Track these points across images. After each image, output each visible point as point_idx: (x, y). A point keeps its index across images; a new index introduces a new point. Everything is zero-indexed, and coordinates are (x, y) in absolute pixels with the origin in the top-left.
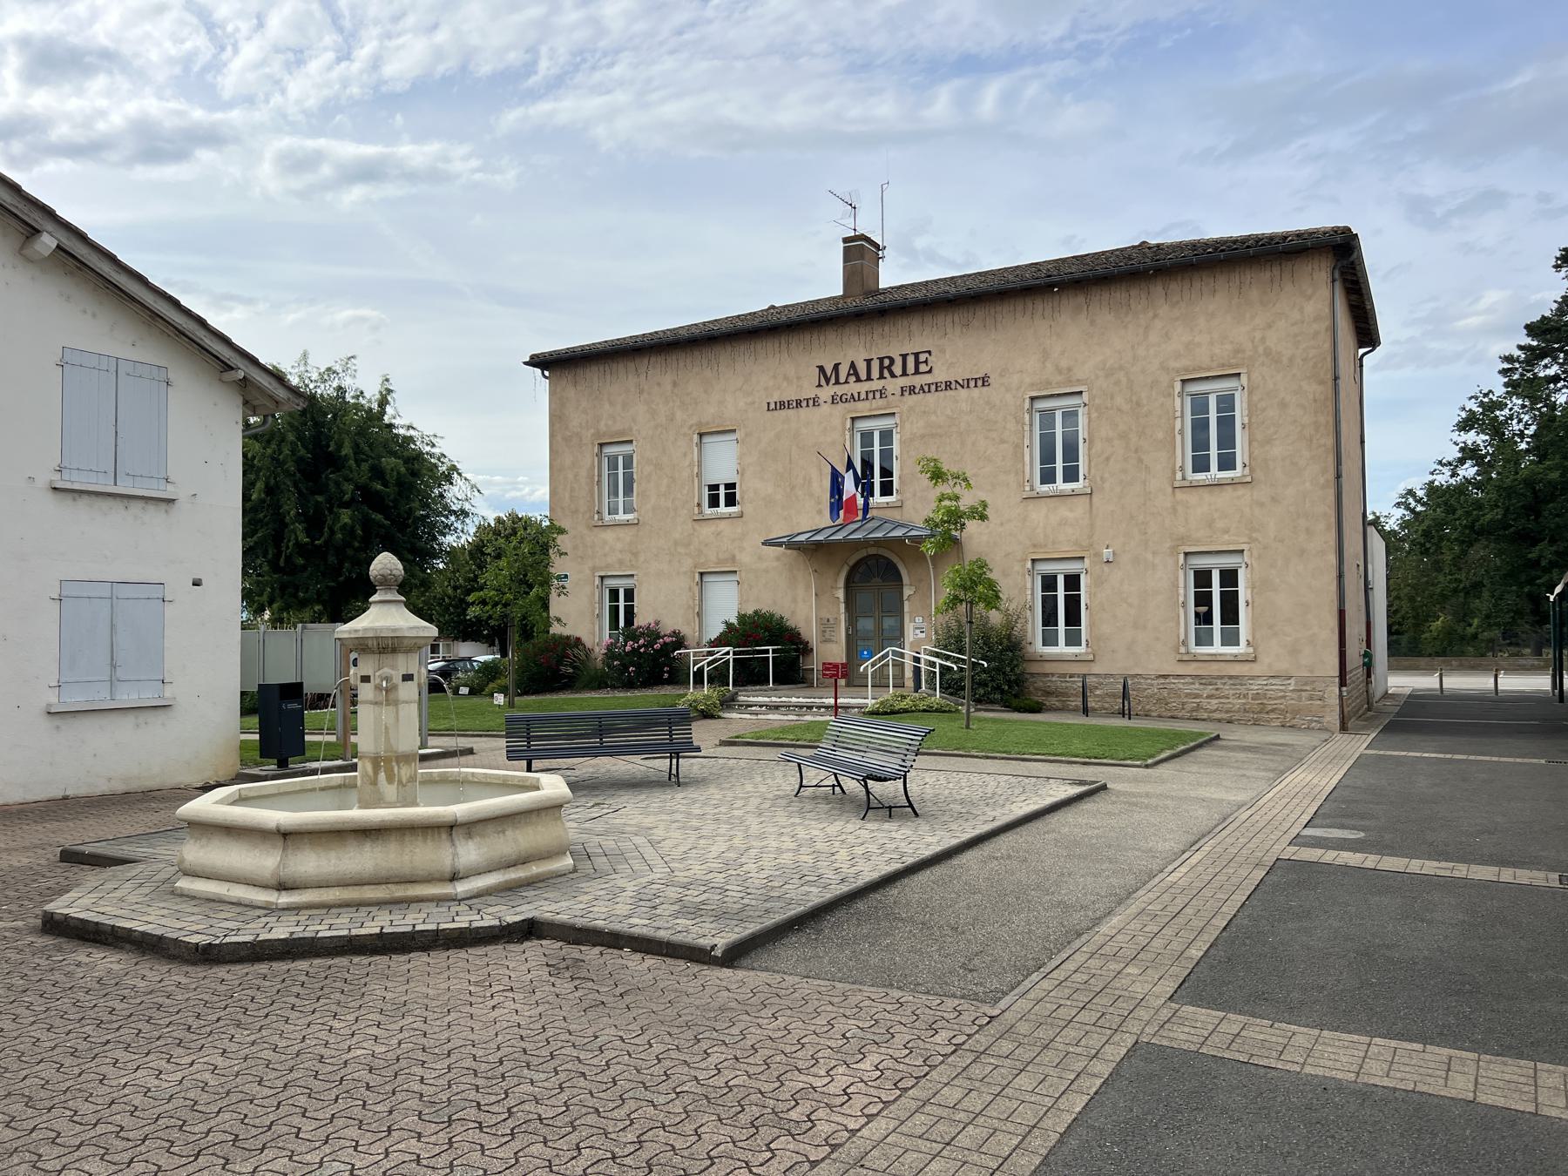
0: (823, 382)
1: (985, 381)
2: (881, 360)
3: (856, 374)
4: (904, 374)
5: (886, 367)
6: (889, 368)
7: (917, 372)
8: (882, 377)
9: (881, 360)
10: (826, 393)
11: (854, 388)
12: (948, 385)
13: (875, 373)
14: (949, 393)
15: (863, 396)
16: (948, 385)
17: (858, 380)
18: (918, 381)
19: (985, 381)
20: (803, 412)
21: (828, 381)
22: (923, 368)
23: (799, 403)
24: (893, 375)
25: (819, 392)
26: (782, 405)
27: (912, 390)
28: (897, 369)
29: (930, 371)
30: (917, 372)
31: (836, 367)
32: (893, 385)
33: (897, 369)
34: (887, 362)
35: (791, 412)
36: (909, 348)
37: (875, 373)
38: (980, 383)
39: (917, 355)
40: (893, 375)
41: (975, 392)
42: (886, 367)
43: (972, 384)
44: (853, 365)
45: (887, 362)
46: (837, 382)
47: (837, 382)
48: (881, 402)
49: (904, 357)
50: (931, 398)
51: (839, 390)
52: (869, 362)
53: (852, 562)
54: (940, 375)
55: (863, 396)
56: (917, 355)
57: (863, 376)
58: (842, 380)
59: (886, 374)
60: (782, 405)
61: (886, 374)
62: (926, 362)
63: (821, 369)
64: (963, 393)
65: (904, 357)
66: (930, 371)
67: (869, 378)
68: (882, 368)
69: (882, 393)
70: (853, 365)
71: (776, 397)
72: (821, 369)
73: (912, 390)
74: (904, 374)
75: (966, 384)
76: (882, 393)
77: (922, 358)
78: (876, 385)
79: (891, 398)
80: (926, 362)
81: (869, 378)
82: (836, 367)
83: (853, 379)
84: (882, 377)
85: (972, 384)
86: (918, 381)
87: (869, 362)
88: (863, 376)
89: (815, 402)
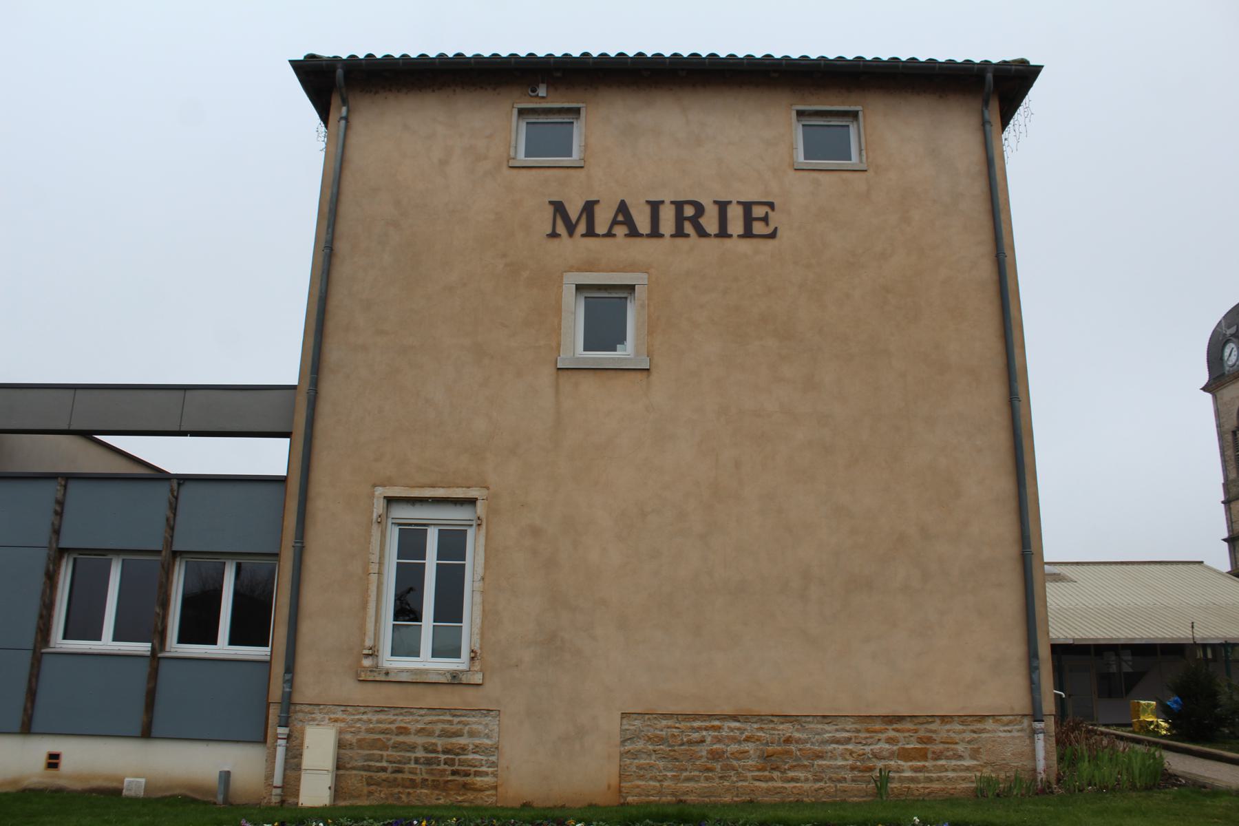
0: (561, 229)
2: (679, 206)
3: (629, 222)
6: (695, 221)
7: (748, 234)
8: (679, 233)
9: (679, 206)
17: (634, 233)
21: (571, 228)
22: (758, 228)
24: (702, 233)
28: (710, 222)
30: (748, 234)
33: (710, 222)
34: (689, 211)
39: (747, 207)
40: (702, 233)
44: (623, 208)
45: (689, 211)
47: (590, 233)
49: (723, 206)
52: (655, 206)
56: (747, 207)
57: (643, 225)
58: (601, 228)
59: (688, 228)
61: (688, 228)
62: (765, 219)
65: (723, 206)
66: (773, 235)
68: (680, 219)
70: (623, 208)
72: (559, 208)
77: (758, 212)
83: (620, 231)
84: (679, 233)
87: (655, 206)
88: (643, 225)
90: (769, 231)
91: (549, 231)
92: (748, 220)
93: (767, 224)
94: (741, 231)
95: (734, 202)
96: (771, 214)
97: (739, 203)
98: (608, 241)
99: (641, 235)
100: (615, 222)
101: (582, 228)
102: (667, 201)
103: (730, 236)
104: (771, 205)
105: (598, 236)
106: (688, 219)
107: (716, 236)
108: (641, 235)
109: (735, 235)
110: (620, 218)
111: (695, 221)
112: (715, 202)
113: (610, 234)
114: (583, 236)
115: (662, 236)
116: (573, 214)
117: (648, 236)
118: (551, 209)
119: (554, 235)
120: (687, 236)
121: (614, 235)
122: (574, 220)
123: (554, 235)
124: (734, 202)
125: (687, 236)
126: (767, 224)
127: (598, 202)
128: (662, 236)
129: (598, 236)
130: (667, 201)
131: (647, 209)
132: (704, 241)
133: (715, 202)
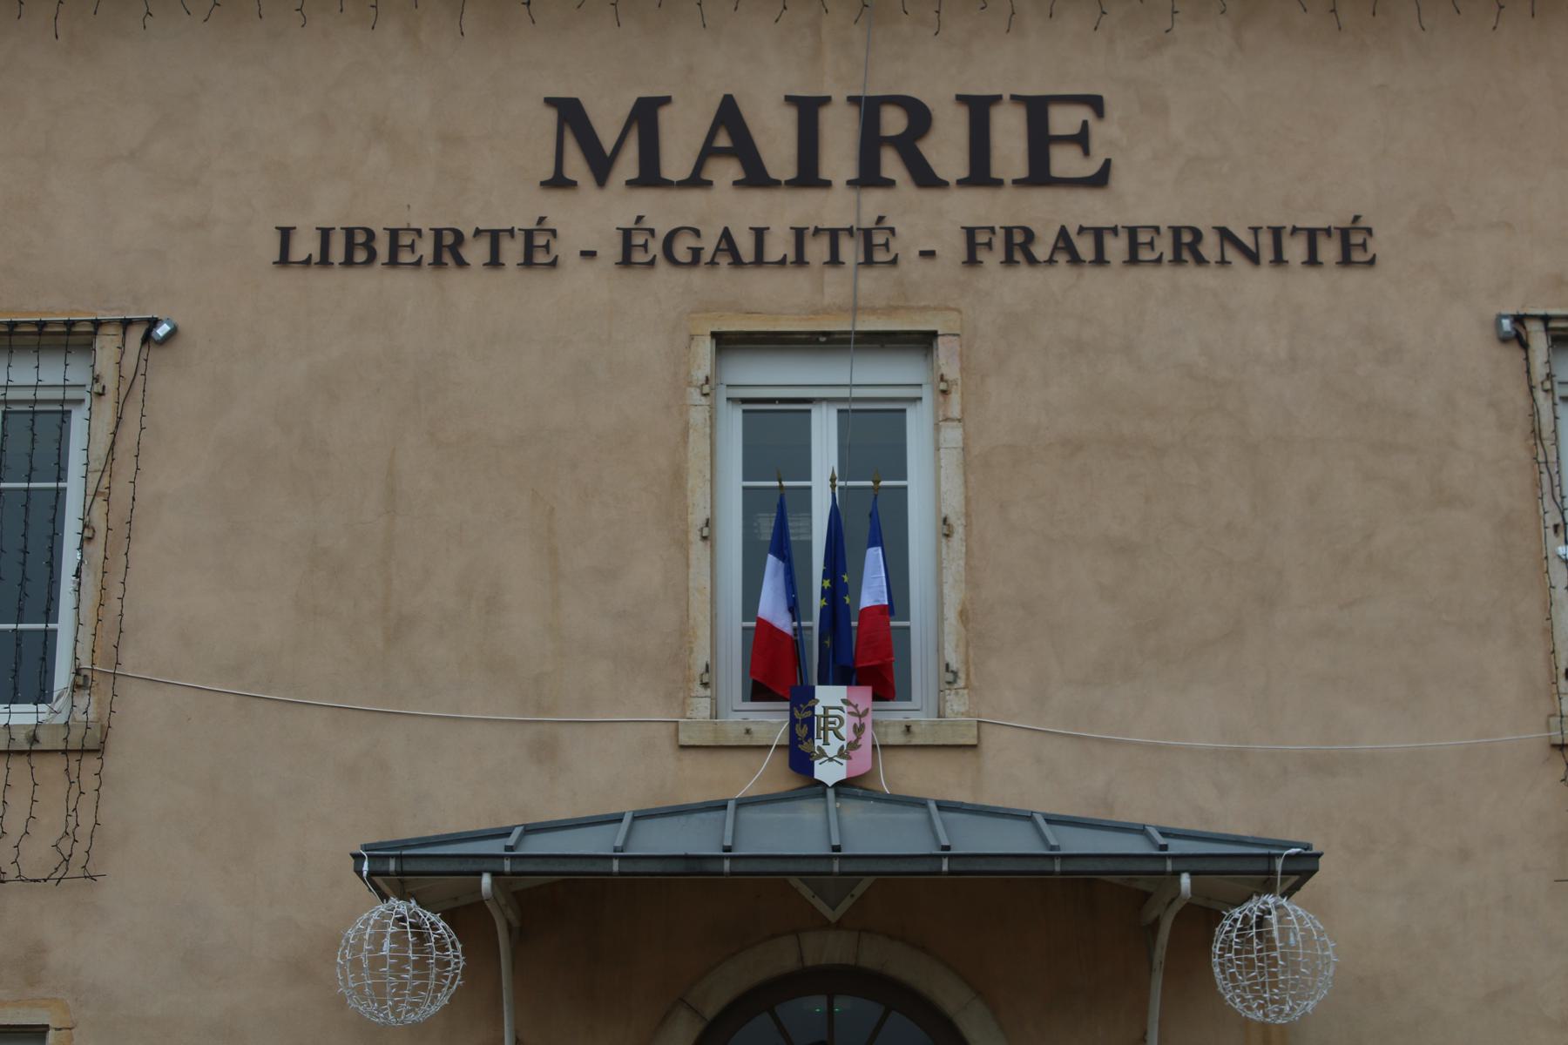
0: (576, 167)
1: (1351, 244)
2: (869, 108)
4: (980, 175)
5: (893, 140)
6: (908, 147)
7: (1039, 175)
8: (869, 177)
9: (869, 108)
10: (594, 215)
11: (728, 206)
12: (1186, 246)
13: (839, 158)
14: (1190, 275)
15: (780, 246)
16: (1186, 246)
17: (756, 177)
18: (1045, 212)
19: (1351, 244)
20: (467, 288)
21: (601, 166)
22: (1065, 161)
23: (448, 249)
24: (925, 177)
25: (555, 208)
26: (358, 247)
27: (1018, 246)
28: (947, 150)
29: (1100, 180)
30: (1039, 175)
31: (646, 115)
32: (927, 220)
33: (947, 150)
34: (894, 122)
35: (402, 280)
36: (1013, 66)
37: (839, 158)
38: (1329, 251)
39: (1037, 109)
40: (925, 177)
41: (1315, 289)
42: (893, 140)
43: (1295, 250)
44: (729, 115)
45: (894, 122)
46: (650, 176)
47: (650, 176)
48: (872, 283)
49: (979, 109)
50: (1107, 291)
51: (661, 211)
52: (808, 110)
53: (717, 995)
54: (1145, 197)
55: (780, 246)
56: (1037, 109)
57: (780, 156)
58: (676, 160)
59: (891, 164)
60: (358, 247)
61: (891, 164)
62: (1081, 139)
63: (570, 114)
64: (1256, 283)
65: (979, 109)
66: (1100, 180)
67: (808, 176)
68: (870, 143)
69: (873, 244)
70: (729, 115)
71: (332, 207)
72: (570, 114)
73: (1018, 246)
74: (980, 175)
75: (1259, 248)
76: (873, 244)
77: (1063, 120)
78: (836, 207)
79: (911, 267)
80: (1081, 139)
81: (808, 176)
82: (646, 115)
83: (726, 172)
84: (869, 177)
85: (1295, 250)
86: (1045, 212)
87: (808, 110)
88: (780, 156)
89: (536, 248)
90: (1091, 168)
91: (547, 172)
92: (1040, 142)
93: (1086, 152)
94: (1021, 170)
95: (1006, 97)
96: (1098, 131)
97: (1015, 98)
98: (695, 197)
99: (775, 184)
100: (709, 151)
101: (628, 165)
102: (839, 94)
103: (998, 183)
104: (1095, 103)
105: (667, 184)
106: (895, 142)
107: (961, 183)
108: (775, 184)
109: (1008, 181)
110: (723, 141)
111: (908, 147)
112: (961, 99)
113: (696, 181)
114: (630, 183)
115: (827, 184)
116: (608, 125)
117: (791, 184)
118: (551, 116)
119: (559, 181)
120: (890, 184)
121: (709, 184)
122: (608, 145)
123: (559, 181)
124: (1006, 97)
125: (890, 184)
126: (1086, 152)
127: (666, 100)
128: (827, 184)
129: (667, 184)
130: (839, 94)
131: (791, 114)
132: (930, 196)
133: (961, 99)
